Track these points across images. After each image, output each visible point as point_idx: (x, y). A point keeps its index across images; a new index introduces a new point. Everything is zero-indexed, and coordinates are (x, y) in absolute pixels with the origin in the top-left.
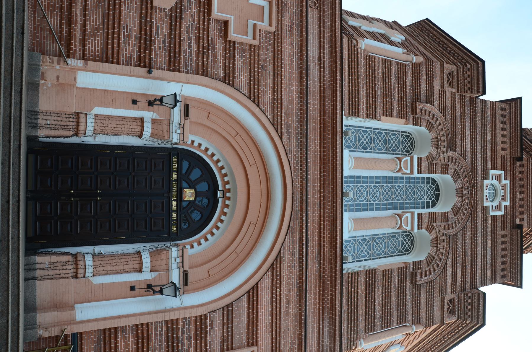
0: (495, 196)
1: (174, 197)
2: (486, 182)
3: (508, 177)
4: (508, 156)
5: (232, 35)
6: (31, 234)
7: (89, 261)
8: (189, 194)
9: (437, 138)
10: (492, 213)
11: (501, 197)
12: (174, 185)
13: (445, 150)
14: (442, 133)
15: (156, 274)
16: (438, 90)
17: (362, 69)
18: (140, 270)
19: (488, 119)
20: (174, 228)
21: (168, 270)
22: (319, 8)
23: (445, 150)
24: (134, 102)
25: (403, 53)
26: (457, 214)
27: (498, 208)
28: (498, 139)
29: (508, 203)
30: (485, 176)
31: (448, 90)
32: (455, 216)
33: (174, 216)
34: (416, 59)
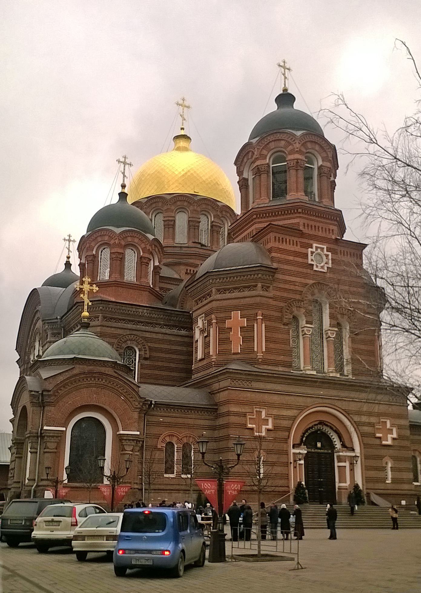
0: (320, 255)
1: (319, 451)
2: (315, 268)
3: (311, 242)
5: (270, 426)
6: (319, 503)
7: (342, 484)
8: (319, 445)
10: (330, 266)
12: (316, 450)
15: (347, 460)
17: (272, 357)
18: (345, 466)
19: (283, 256)
20: (330, 451)
21: (346, 456)
25: (257, 323)
27: (327, 256)
28: (292, 249)
31: (272, 293)
33: (326, 451)
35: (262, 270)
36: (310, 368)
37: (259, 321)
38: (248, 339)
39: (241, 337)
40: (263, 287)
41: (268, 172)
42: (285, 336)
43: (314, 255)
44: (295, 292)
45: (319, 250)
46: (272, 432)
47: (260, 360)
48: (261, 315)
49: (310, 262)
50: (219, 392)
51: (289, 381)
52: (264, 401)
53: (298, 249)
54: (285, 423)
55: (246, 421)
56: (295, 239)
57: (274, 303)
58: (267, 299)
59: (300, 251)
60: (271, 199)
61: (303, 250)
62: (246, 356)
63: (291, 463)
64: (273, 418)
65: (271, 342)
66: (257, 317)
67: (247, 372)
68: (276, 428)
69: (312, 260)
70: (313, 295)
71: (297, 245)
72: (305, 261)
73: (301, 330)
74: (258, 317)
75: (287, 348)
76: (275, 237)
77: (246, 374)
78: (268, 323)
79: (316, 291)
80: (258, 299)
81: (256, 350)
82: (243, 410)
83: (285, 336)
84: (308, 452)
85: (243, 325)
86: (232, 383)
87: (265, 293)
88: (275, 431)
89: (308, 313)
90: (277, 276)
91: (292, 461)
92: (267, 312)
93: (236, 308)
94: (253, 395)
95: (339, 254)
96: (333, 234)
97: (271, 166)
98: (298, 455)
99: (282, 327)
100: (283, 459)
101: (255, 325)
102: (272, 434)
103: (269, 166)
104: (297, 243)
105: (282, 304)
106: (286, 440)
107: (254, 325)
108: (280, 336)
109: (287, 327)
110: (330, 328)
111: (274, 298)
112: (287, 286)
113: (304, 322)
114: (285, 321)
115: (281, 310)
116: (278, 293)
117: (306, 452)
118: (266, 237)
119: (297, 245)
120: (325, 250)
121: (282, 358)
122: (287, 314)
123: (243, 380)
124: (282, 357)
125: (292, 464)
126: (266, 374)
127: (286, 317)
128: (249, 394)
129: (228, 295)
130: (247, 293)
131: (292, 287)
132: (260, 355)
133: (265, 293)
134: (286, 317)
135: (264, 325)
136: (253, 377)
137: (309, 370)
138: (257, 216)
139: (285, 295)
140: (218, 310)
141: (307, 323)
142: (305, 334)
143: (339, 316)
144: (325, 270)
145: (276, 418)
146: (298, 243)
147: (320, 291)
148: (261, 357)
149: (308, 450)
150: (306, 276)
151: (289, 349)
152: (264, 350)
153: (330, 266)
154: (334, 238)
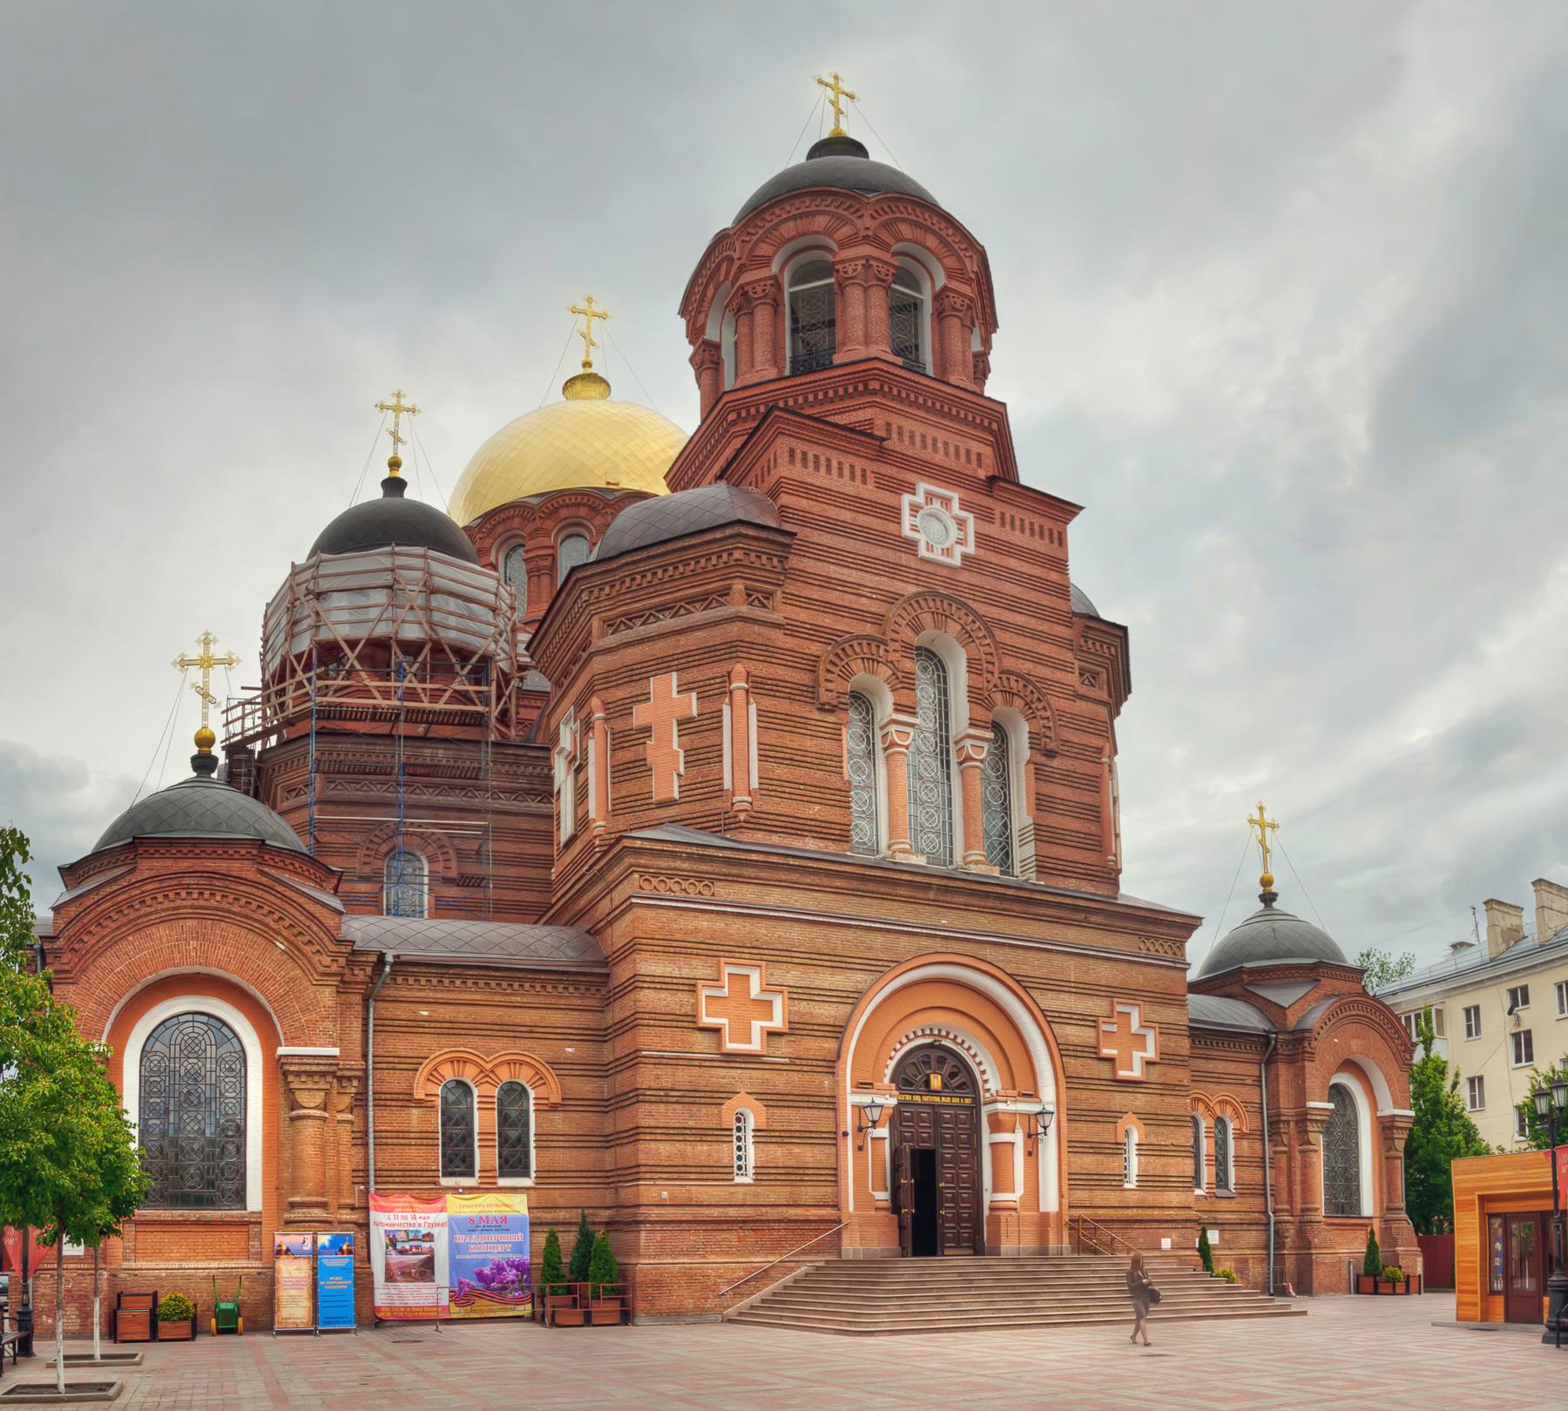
2: (923, 551)
4: (875, 466)
5: (777, 1023)
9: (863, 659)
10: (971, 549)
11: (944, 510)
13: (882, 647)
14: (857, 648)
16: (788, 639)
17: (785, 807)
22: (712, 880)
23: (882, 647)
24: (860, 1148)
25: (731, 704)
26: (970, 636)
27: (961, 523)
29: (955, 496)
30: (911, 546)
32: (973, 641)
34: (739, 680)
35: (746, 536)
36: (907, 846)
37: (739, 697)
38: (703, 755)
39: (682, 753)
40: (749, 595)
41: (776, 305)
42: (828, 746)
43: (919, 515)
44: (859, 615)
45: (937, 504)
46: (784, 1039)
47: (742, 816)
48: (745, 675)
49: (907, 531)
50: (611, 923)
51: (838, 883)
52: (755, 944)
53: (869, 491)
54: (827, 1012)
55: (696, 1006)
56: (860, 464)
57: (790, 642)
58: (762, 630)
59: (873, 498)
60: (787, 372)
61: (886, 497)
62: (697, 807)
63: (845, 1134)
64: (786, 994)
65: (780, 761)
66: (730, 684)
67: (694, 850)
68: (796, 1028)
69: (914, 528)
70: (917, 628)
71: (864, 482)
72: (891, 527)
73: (879, 734)
74: (734, 685)
75: (834, 781)
76: (792, 451)
77: (690, 857)
78: (767, 703)
79: (927, 618)
80: (735, 630)
81: (727, 784)
82: (686, 972)
83: (828, 746)
84: (900, 1104)
85: (687, 714)
86: (646, 885)
87: (758, 613)
88: (793, 1038)
89: (904, 682)
90: (794, 562)
91: (850, 1131)
92: (761, 669)
93: (663, 665)
94: (720, 924)
95: (998, 522)
96: (981, 467)
97: (787, 290)
98: (868, 1110)
99: (817, 715)
100: (818, 1120)
101: (726, 710)
102: (784, 1048)
103: (780, 288)
104: (864, 476)
105: (815, 648)
106: (830, 1065)
107: (721, 711)
108: (810, 744)
109: (831, 718)
110: (973, 731)
111: (789, 628)
112: (833, 596)
113: (889, 708)
114: (825, 697)
115: (812, 665)
116: (803, 615)
117: (894, 1102)
118: (764, 458)
119: (864, 482)
120: (956, 504)
121: (815, 811)
122: (829, 676)
123: (686, 878)
124: (817, 807)
125: (850, 1138)
126: (761, 858)
127: (830, 685)
128: (704, 923)
129: (640, 630)
130: (698, 615)
131: (848, 600)
132: (740, 800)
133: (758, 613)
134: (830, 685)
135: (753, 709)
136: (715, 868)
137: (904, 851)
138: (739, 415)
139: (827, 621)
140: (612, 678)
141: (898, 708)
142: (893, 744)
143: (998, 697)
144: (957, 561)
145: (797, 994)
146: (868, 473)
147: (941, 619)
148: (746, 806)
149: (902, 1098)
150: (895, 571)
151: (839, 785)
152: (755, 784)
153: (971, 549)
154: (983, 477)
